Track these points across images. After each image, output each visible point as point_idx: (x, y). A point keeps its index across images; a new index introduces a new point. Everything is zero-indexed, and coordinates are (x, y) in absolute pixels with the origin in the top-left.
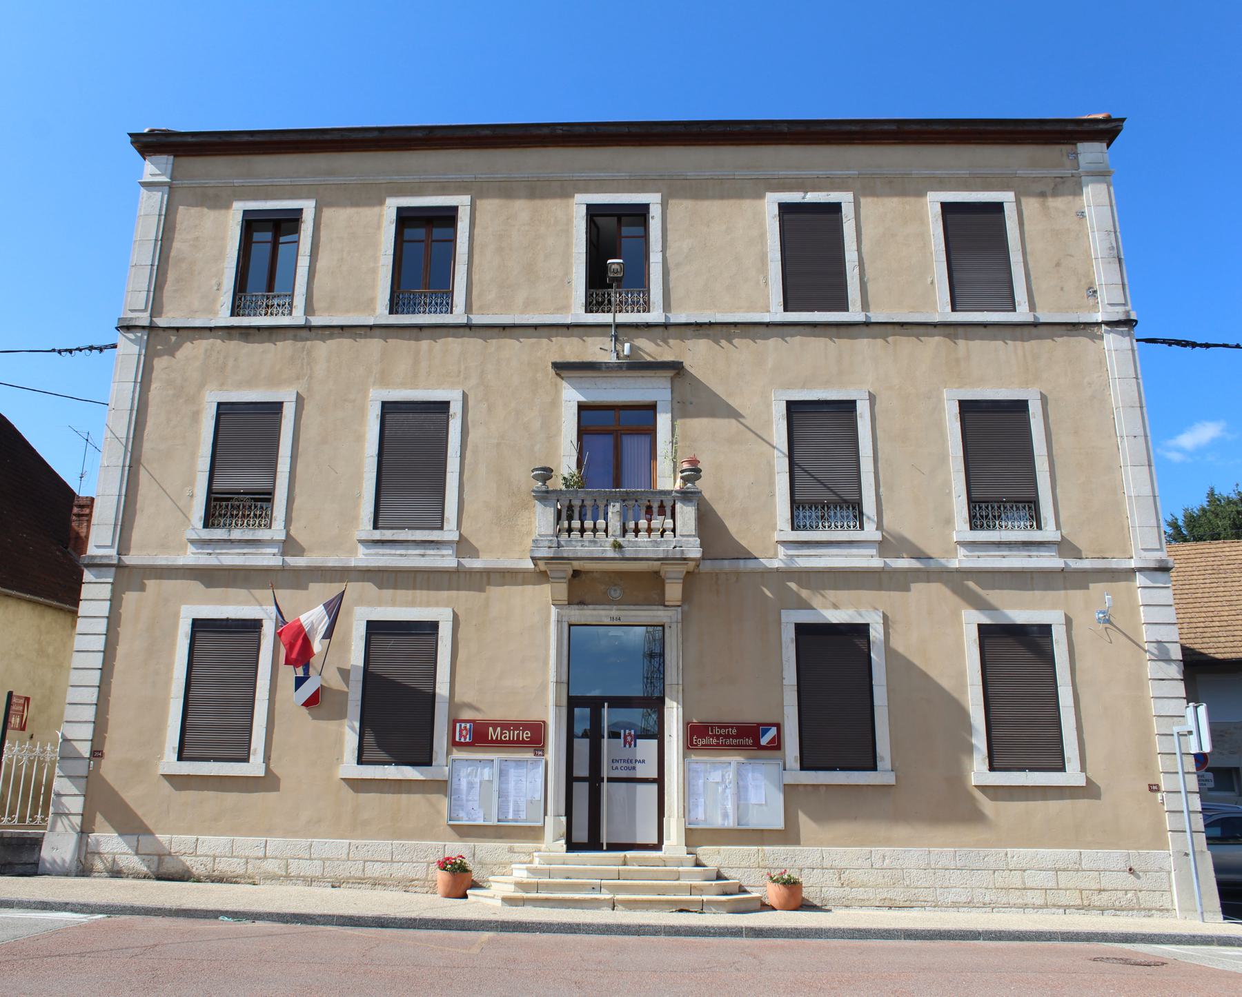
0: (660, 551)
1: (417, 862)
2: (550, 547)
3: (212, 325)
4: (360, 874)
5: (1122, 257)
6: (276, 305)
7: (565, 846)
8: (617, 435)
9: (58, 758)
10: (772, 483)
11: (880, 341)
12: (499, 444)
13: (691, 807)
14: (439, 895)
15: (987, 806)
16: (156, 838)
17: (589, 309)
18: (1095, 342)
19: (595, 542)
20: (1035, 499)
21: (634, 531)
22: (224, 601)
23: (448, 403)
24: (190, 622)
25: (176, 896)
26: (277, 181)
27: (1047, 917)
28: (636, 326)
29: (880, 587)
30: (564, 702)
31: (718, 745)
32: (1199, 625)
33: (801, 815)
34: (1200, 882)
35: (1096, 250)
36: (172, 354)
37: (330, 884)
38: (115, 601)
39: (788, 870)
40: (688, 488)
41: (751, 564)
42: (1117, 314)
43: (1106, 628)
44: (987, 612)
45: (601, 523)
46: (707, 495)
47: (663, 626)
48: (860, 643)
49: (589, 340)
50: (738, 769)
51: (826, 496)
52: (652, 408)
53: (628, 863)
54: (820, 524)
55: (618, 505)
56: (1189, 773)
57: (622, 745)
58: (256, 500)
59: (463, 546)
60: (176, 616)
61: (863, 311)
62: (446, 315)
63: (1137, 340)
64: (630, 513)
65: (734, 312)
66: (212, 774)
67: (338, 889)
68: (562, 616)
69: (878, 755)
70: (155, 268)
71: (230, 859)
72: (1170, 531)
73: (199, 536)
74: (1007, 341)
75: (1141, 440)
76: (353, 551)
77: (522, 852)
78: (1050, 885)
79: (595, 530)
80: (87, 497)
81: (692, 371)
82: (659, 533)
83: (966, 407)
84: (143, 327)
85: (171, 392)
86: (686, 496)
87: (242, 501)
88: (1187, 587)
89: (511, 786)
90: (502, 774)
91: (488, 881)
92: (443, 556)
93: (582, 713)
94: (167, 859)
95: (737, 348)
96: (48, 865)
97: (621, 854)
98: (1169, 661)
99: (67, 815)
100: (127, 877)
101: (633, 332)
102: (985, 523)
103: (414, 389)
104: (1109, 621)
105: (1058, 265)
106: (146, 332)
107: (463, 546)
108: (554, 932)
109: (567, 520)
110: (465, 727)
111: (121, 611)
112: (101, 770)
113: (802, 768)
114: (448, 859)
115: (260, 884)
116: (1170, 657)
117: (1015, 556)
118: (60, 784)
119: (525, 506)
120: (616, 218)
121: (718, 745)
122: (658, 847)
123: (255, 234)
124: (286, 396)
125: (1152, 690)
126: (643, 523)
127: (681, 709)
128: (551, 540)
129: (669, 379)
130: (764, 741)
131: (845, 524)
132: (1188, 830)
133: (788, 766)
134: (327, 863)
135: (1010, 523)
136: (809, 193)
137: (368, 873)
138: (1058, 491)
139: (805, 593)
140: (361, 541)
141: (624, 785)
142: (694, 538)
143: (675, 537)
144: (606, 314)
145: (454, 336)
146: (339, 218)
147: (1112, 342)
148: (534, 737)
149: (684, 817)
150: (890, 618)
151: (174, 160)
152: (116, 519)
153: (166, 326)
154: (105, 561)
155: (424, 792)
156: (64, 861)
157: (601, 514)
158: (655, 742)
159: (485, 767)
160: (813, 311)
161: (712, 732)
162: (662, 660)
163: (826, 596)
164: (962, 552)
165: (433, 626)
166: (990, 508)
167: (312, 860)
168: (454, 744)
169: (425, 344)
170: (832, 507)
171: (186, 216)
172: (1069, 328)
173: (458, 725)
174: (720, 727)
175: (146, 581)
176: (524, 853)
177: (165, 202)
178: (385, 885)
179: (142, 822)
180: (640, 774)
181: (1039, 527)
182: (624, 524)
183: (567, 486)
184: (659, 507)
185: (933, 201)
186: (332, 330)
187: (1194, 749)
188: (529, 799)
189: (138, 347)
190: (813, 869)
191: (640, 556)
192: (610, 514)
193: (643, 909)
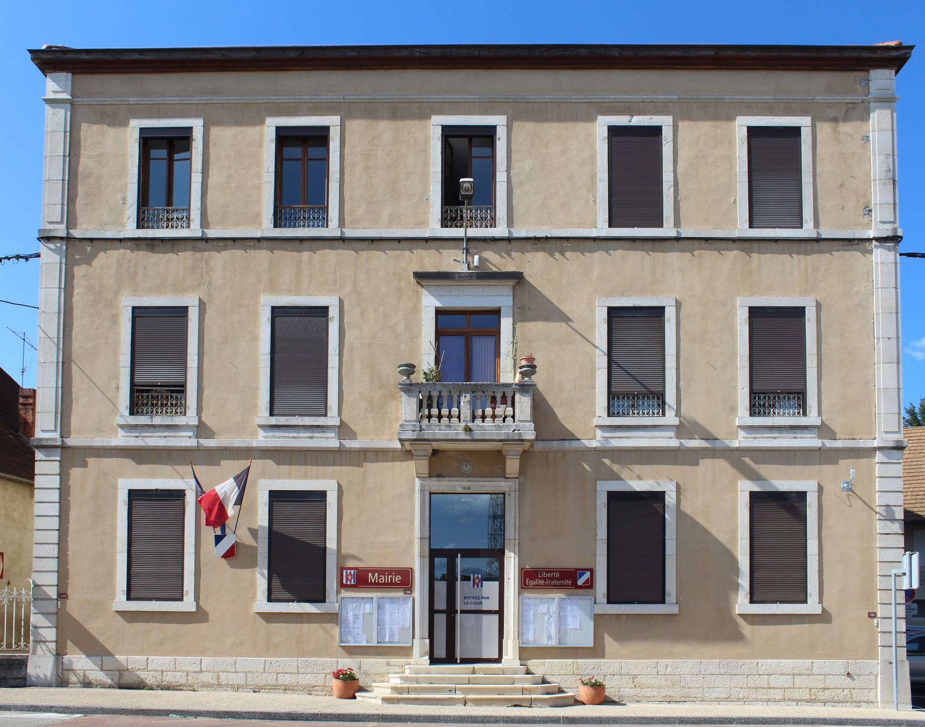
0: (503, 434)
1: (317, 673)
2: (413, 431)
3: (122, 237)
4: (274, 682)
5: (897, 179)
6: (175, 219)
7: (428, 661)
8: (468, 336)
9: (32, 600)
10: (593, 377)
11: (688, 254)
12: (370, 344)
13: (524, 631)
14: (334, 697)
15: (746, 629)
16: (116, 659)
17: (445, 223)
18: (865, 256)
19: (450, 426)
20: (802, 391)
21: (481, 418)
22: (153, 475)
23: (327, 308)
24: (127, 492)
25: (135, 700)
26: (168, 100)
27: (784, 707)
28: (484, 240)
29: (675, 463)
30: (427, 553)
31: (545, 585)
32: (919, 493)
34: (899, 682)
35: (875, 172)
37: (252, 690)
38: (64, 475)
39: (595, 676)
40: (525, 382)
41: (575, 444)
42: (886, 231)
44: (757, 482)
45: (455, 411)
46: (540, 387)
48: (657, 506)
49: (445, 252)
50: (560, 603)
51: (637, 388)
52: (497, 313)
54: (631, 412)
55: (468, 396)
56: (899, 604)
57: (472, 586)
59: (344, 430)
60: (115, 487)
61: (674, 227)
62: (323, 229)
63: (901, 255)
64: (479, 402)
65: (567, 228)
66: (155, 610)
68: (424, 486)
69: (666, 592)
70: (66, 182)
71: (174, 673)
72: (908, 417)
73: (127, 422)
74: (793, 255)
75: (894, 342)
76: (254, 434)
77: (396, 666)
78: (788, 685)
79: (450, 416)
80: (30, 389)
81: (530, 280)
82: (502, 419)
83: (755, 313)
84: (62, 238)
85: (91, 298)
86: (524, 388)
88: (915, 463)
89: (387, 617)
90: (380, 608)
91: (371, 686)
92: (328, 438)
93: (441, 562)
94: (126, 673)
95: (568, 260)
96: (34, 679)
97: (471, 666)
98: (893, 520)
99: (44, 642)
100: (96, 687)
101: (481, 245)
102: (762, 410)
103: (298, 295)
104: (851, 490)
105: (842, 186)
106: (64, 242)
107: (344, 430)
108: (421, 722)
109: (428, 408)
110: (350, 573)
111: (69, 483)
113: (609, 602)
114: (340, 671)
115: (198, 691)
116: (894, 517)
117: (784, 438)
118: (35, 619)
119: (393, 397)
120: (467, 139)
121: (545, 585)
122: (498, 660)
123: (152, 151)
124: (190, 300)
125: (879, 542)
126: (489, 411)
127: (517, 559)
128: (414, 425)
130: (580, 582)
131: (651, 411)
132: (894, 646)
133: (597, 601)
134: (249, 675)
135: (782, 411)
136: (634, 117)
137: (280, 682)
138: (823, 384)
139: (616, 467)
140: (260, 426)
141: (473, 615)
142: (529, 423)
143: (514, 422)
145: (331, 248)
146: (224, 135)
147: (881, 256)
148: (404, 580)
149: (518, 638)
150: (682, 487)
151: (72, 78)
152: (56, 407)
153: (81, 237)
155: (320, 622)
156: (46, 676)
157: (455, 403)
158: (497, 583)
159: (366, 603)
160: (633, 227)
161: (541, 575)
162: (503, 521)
163: (634, 470)
164: (742, 434)
165: (323, 495)
166: (767, 399)
167: (237, 672)
168: (342, 586)
169: (306, 255)
170: (641, 397)
171: (89, 132)
172: (845, 243)
173: (345, 571)
174: (547, 572)
175: (87, 459)
176: (398, 666)
177: (69, 119)
178: (293, 690)
179: (103, 647)
180: (486, 606)
181: (805, 414)
182: (473, 411)
183: (427, 380)
184: (502, 397)
185: (743, 123)
186: (226, 242)
187: (906, 587)
188: (401, 626)
189: (59, 256)
190: (614, 675)
191: (486, 438)
192: (462, 403)
193: (487, 705)
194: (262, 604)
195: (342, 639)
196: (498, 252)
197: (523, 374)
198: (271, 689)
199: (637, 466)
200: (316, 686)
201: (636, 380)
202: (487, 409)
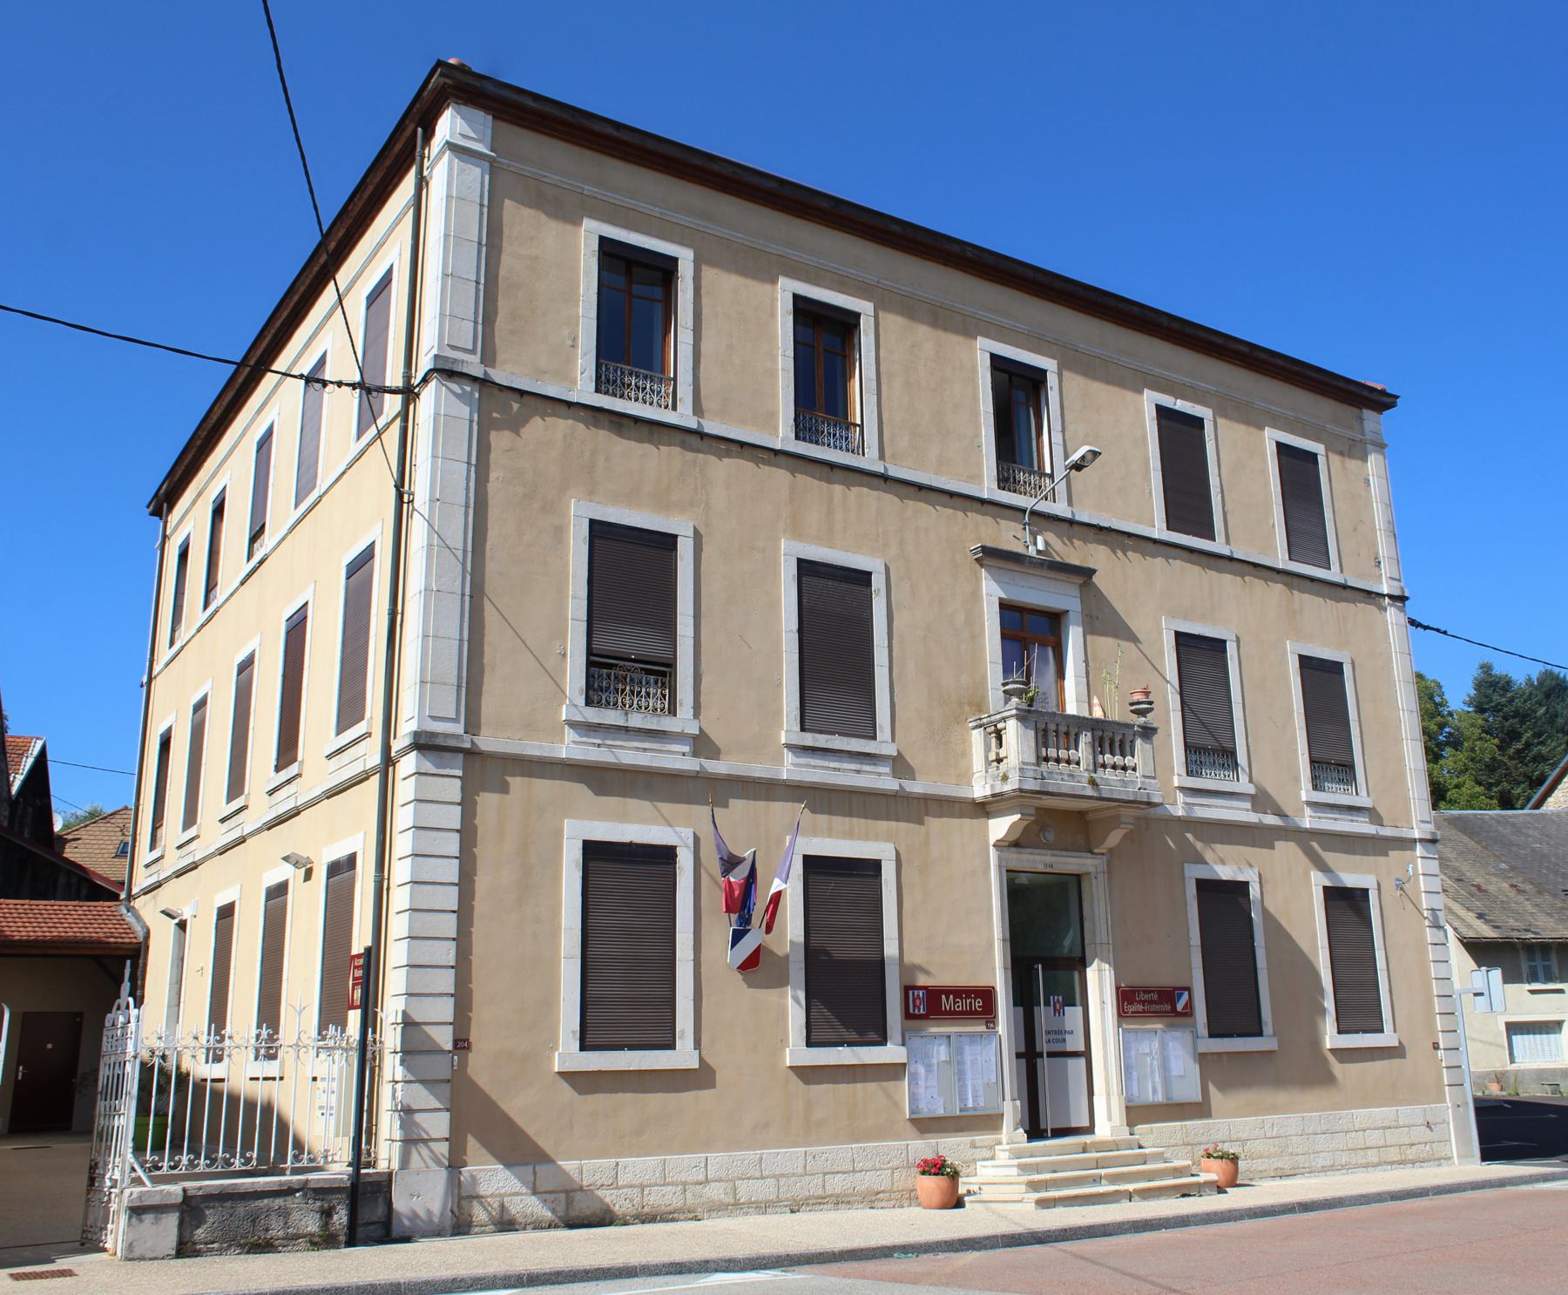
4: (820, 1192)
11: (1239, 579)
15: (1337, 1068)
16: (559, 1167)
22: (623, 817)
31: (1144, 1012)
33: (1210, 1083)
36: (516, 430)
43: (1401, 895)
49: (1003, 522)
53: (1088, 1150)
58: (648, 672)
60: (558, 834)
66: (631, 1069)
67: (798, 1213)
71: (662, 1188)
73: (585, 718)
87: (629, 671)
92: (879, 774)
94: (578, 1196)
96: (406, 1222)
99: (425, 1141)
100: (525, 1229)
106: (477, 386)
110: (918, 995)
112: (469, 1069)
113: (1211, 1035)
115: (703, 1219)
124: (678, 525)
127: (1112, 972)
137: (829, 1191)
139: (1199, 845)
144: (1022, 496)
146: (725, 285)
152: (459, 677)
153: (505, 384)
154: (452, 743)
156: (429, 1212)
159: (941, 1045)
168: (908, 1016)
173: (911, 993)
175: (509, 779)
178: (849, 1202)
179: (535, 1145)
189: (469, 408)
194: (797, 1052)
196: (1059, 536)
198: (816, 1204)
199: (1220, 845)
200: (879, 1193)
201: (1208, 730)
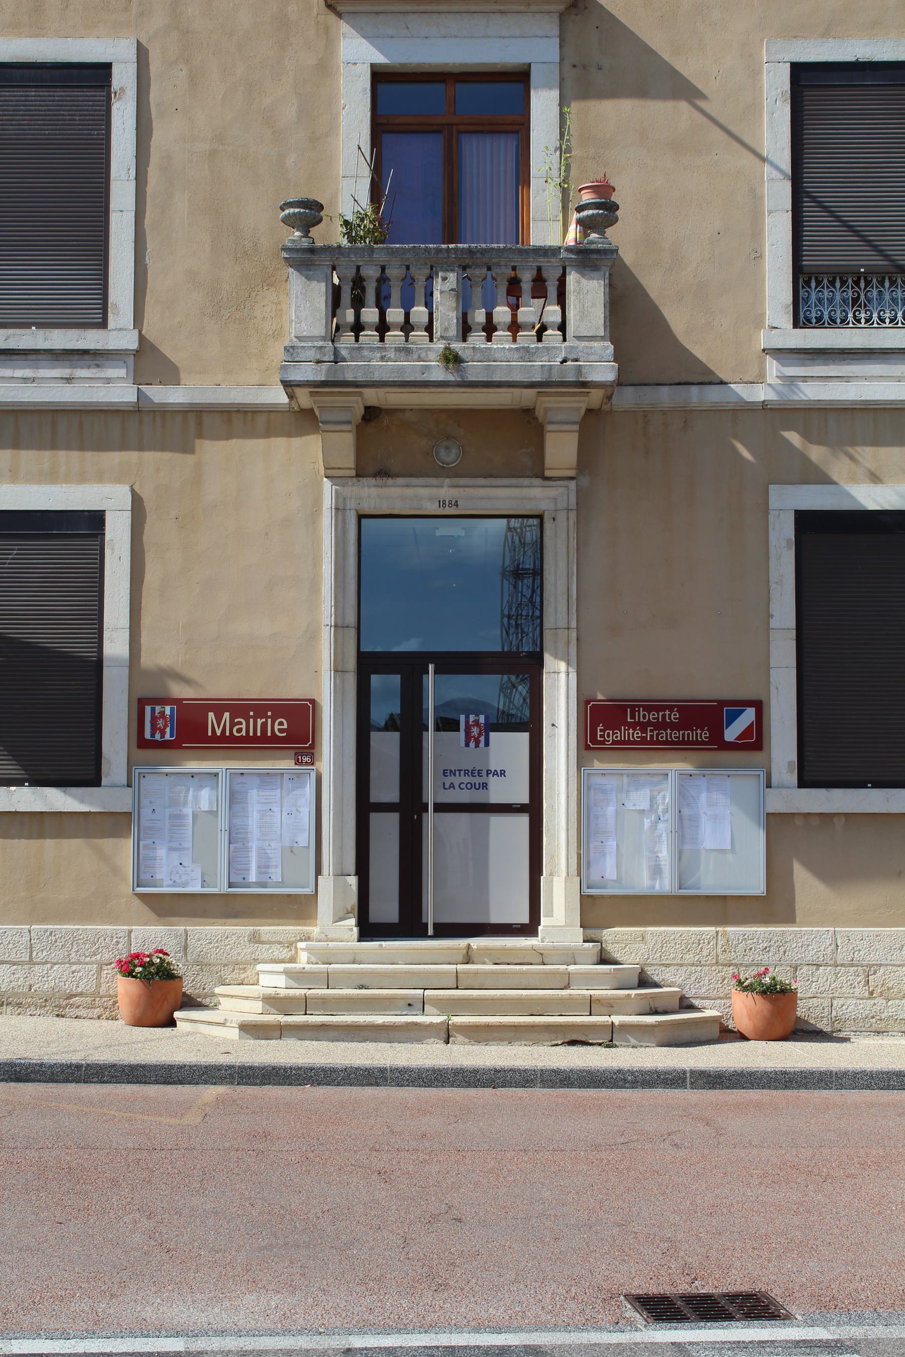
1: (79, 963)
7: (356, 930)
10: (757, 233)
12: (213, 154)
13: (592, 856)
14: (121, 1022)
21: (484, 330)
31: (643, 741)
39: (771, 969)
40: (592, 242)
41: (713, 395)
45: (419, 312)
46: (628, 256)
47: (540, 517)
50: (681, 786)
51: (865, 260)
53: (475, 958)
54: (850, 315)
55: (452, 277)
57: (463, 744)
64: (478, 292)
79: (407, 327)
82: (534, 333)
89: (253, 820)
90: (235, 799)
91: (213, 995)
92: (108, 380)
97: (462, 943)
109: (352, 307)
113: (803, 783)
114: (137, 956)
119: (269, 281)
121: (643, 741)
122: (530, 929)
126: (502, 313)
127: (573, 676)
128: (321, 348)
129: (555, 19)
130: (731, 734)
133: (775, 780)
139: (816, 453)
141: (465, 817)
143: (565, 340)
149: (579, 874)
155: (86, 834)
157: (420, 294)
158: (524, 737)
159: (201, 787)
161: (633, 717)
162: (537, 582)
163: (860, 459)
170: (874, 280)
176: (280, 943)
180: (497, 793)
182: (465, 315)
183: (351, 240)
190: (818, 966)
191: (497, 378)
192: (437, 295)
195: (142, 877)
197: (586, 225)
202: (498, 309)
